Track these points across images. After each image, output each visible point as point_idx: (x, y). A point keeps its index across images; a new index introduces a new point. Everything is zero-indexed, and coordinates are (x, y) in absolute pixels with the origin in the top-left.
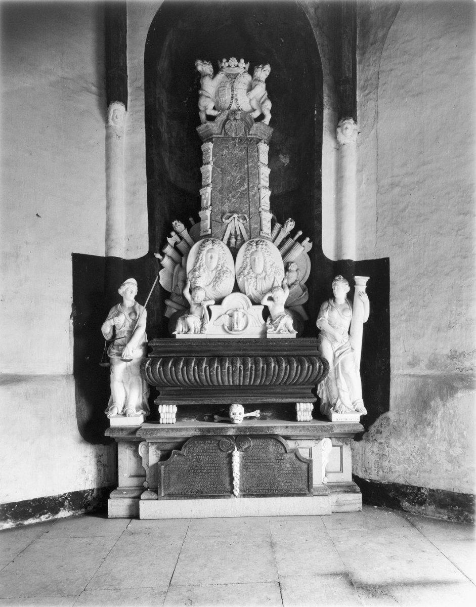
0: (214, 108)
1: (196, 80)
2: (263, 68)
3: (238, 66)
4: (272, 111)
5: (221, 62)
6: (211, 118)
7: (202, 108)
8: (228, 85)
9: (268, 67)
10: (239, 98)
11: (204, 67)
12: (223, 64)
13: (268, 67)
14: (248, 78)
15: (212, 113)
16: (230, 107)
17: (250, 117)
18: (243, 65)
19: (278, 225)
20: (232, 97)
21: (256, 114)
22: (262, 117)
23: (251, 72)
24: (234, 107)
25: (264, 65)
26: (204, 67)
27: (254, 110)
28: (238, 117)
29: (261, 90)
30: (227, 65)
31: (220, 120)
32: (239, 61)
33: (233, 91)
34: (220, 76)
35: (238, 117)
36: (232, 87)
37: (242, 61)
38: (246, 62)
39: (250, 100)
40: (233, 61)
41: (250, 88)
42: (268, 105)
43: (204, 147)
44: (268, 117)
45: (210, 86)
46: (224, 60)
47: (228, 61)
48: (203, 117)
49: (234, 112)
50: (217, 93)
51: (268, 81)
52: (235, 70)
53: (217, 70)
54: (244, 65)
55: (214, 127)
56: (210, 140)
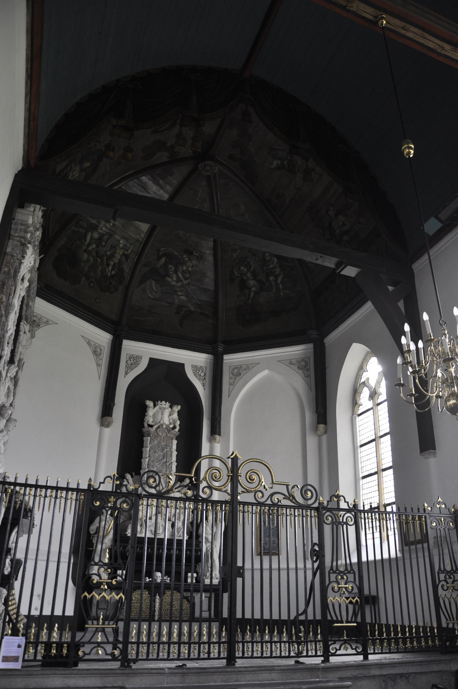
0: (152, 422)
1: (145, 409)
2: (177, 407)
3: (165, 405)
5: (158, 402)
7: (146, 421)
8: (160, 412)
9: (179, 407)
10: (165, 418)
11: (150, 403)
12: (158, 403)
13: (179, 407)
14: (170, 409)
16: (160, 422)
17: (169, 427)
18: (168, 404)
20: (162, 418)
21: (171, 426)
22: (174, 428)
23: (171, 407)
24: (162, 422)
25: (178, 405)
26: (150, 403)
27: (171, 424)
28: (164, 427)
29: (175, 416)
30: (160, 403)
31: (155, 427)
32: (166, 402)
33: (162, 415)
34: (157, 408)
36: (162, 413)
37: (168, 403)
38: (169, 403)
39: (170, 420)
40: (164, 402)
42: (178, 422)
45: (151, 412)
46: (159, 402)
47: (161, 402)
48: (146, 425)
49: (162, 425)
50: (154, 415)
51: (178, 412)
52: (164, 406)
53: (155, 406)
54: (168, 404)
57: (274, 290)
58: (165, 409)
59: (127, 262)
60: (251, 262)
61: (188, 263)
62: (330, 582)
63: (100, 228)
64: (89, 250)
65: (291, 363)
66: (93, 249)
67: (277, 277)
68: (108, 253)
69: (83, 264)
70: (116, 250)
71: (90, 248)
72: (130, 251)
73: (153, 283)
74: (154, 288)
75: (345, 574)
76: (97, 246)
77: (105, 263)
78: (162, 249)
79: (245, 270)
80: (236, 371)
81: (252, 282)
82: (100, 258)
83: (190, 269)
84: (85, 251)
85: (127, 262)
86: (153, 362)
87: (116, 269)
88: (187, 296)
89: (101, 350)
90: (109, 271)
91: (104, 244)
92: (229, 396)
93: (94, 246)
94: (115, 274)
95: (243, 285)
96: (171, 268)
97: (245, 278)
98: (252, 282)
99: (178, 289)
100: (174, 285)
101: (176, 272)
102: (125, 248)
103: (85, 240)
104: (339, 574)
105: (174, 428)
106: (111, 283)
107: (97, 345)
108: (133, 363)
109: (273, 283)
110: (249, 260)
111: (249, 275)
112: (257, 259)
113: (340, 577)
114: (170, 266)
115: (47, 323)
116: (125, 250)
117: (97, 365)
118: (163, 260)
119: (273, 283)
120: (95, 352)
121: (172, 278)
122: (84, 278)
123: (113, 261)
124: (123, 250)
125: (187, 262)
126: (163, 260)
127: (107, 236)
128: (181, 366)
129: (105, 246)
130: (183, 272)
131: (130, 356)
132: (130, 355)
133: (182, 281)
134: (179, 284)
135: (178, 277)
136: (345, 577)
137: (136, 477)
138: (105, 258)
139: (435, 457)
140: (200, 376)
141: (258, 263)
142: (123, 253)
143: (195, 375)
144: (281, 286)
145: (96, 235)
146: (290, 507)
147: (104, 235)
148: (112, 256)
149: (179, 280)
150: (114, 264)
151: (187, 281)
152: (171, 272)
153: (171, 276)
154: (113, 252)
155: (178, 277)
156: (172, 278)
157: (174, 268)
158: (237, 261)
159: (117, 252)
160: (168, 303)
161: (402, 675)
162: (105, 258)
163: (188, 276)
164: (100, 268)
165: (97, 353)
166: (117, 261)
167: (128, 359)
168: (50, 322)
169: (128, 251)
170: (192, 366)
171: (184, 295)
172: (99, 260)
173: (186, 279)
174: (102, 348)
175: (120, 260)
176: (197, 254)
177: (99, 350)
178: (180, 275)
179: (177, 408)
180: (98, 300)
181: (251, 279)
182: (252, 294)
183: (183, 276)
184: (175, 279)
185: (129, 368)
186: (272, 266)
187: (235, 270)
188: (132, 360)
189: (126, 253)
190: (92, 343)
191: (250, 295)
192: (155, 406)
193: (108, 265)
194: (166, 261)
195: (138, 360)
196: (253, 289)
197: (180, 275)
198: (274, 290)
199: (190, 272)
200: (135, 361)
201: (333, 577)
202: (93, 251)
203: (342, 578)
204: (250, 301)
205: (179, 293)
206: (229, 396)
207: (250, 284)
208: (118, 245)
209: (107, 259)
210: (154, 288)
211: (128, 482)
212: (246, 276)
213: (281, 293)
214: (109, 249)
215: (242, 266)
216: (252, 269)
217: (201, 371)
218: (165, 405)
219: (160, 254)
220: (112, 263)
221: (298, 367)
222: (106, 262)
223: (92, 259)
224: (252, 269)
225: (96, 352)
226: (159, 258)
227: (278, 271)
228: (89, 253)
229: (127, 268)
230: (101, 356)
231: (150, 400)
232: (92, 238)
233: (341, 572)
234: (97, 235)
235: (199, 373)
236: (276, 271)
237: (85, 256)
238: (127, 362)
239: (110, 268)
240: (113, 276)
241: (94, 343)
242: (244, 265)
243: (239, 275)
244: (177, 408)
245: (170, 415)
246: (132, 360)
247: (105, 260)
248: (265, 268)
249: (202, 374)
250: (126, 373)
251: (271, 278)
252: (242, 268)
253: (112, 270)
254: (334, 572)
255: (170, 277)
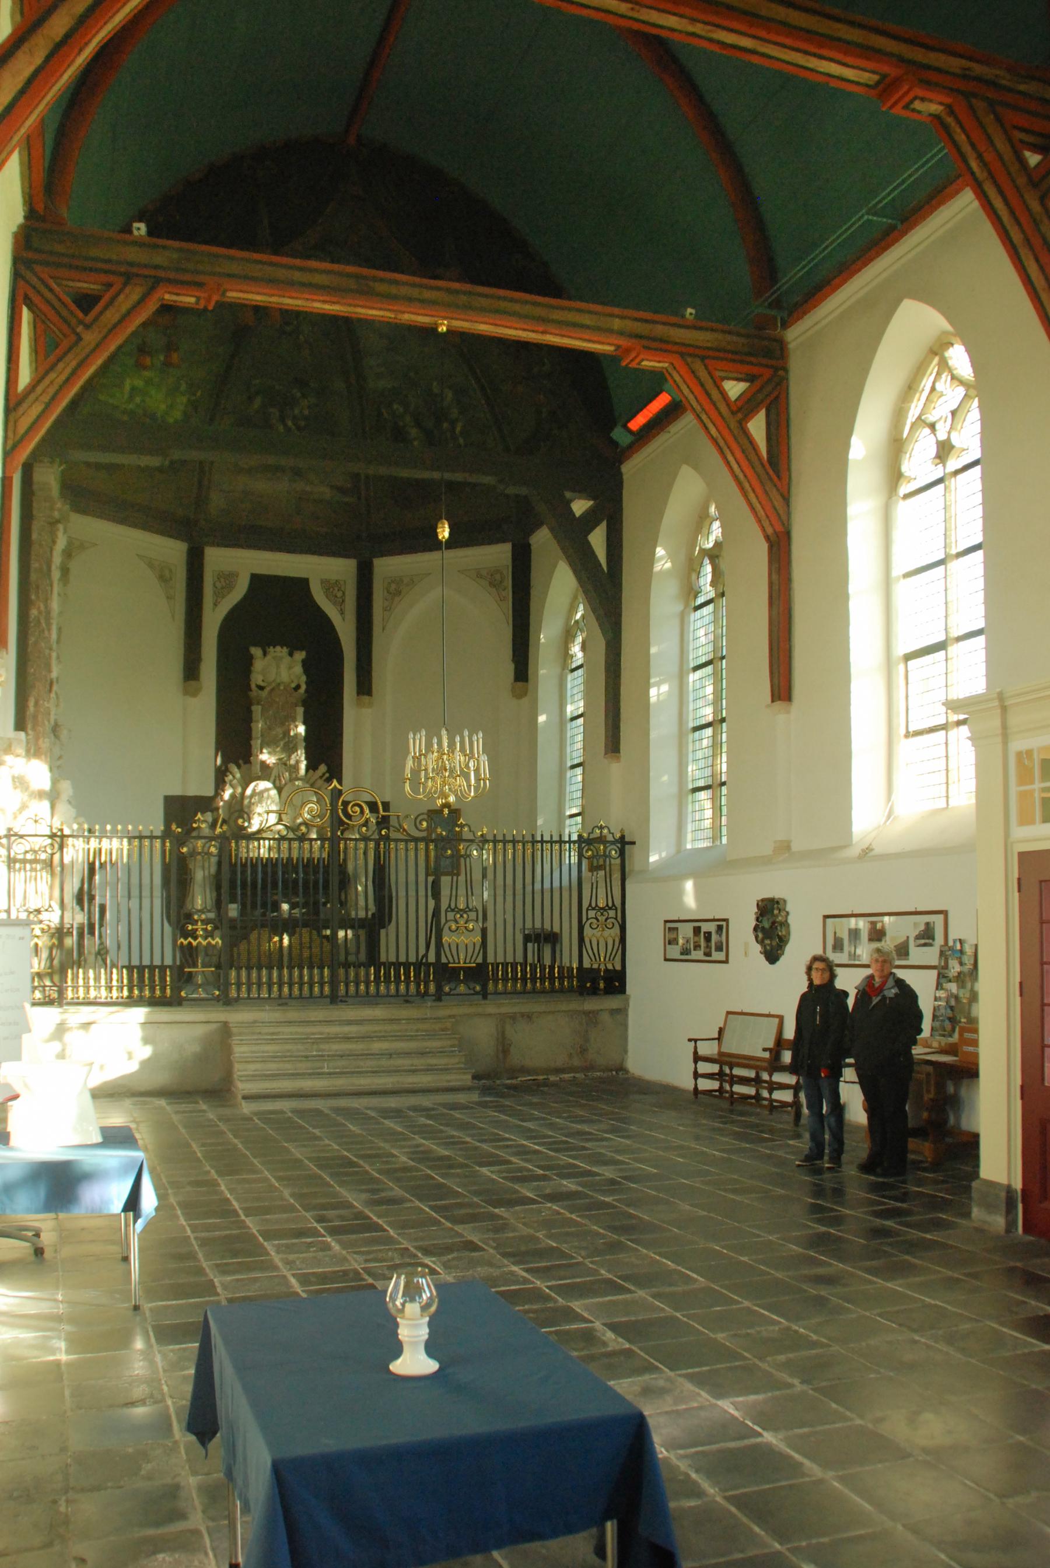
1: (249, 660)
4: (306, 683)
6: (261, 688)
11: (256, 652)
14: (289, 658)
15: (262, 684)
18: (285, 650)
19: (311, 771)
22: (298, 687)
23: (291, 654)
24: (278, 681)
26: (256, 652)
28: (282, 688)
29: (298, 669)
34: (269, 657)
35: (282, 688)
40: (278, 648)
41: (290, 668)
42: (304, 678)
43: (254, 708)
44: (304, 687)
45: (258, 665)
48: (253, 686)
52: (279, 654)
53: (265, 654)
55: (264, 694)
56: (258, 704)
58: (281, 658)
62: (447, 921)
65: (479, 576)
67: (453, 423)
75: (465, 912)
79: (401, 410)
80: (393, 586)
81: (414, 432)
83: (306, 412)
86: (258, 581)
89: (171, 571)
92: (383, 629)
98: (414, 432)
101: (282, 419)
104: (458, 912)
105: (298, 687)
108: (224, 584)
111: (408, 418)
113: (458, 916)
114: (271, 410)
117: (168, 598)
118: (258, 402)
120: (162, 578)
126: (258, 402)
128: (303, 584)
136: (465, 916)
137: (244, 767)
139: (618, 759)
140: (336, 596)
143: (327, 597)
146: (402, 840)
157: (278, 414)
161: (523, 1015)
163: (302, 423)
170: (322, 582)
178: (290, 423)
179: (300, 656)
185: (220, 594)
188: (222, 580)
192: (265, 654)
197: (290, 423)
201: (450, 915)
203: (462, 916)
206: (383, 629)
211: (234, 777)
217: (336, 589)
218: (281, 651)
221: (490, 583)
225: (164, 578)
226: (250, 399)
227: (455, 413)
231: (255, 645)
232: (133, 389)
233: (461, 910)
235: (335, 592)
244: (300, 656)
245: (290, 668)
246: (222, 580)
249: (339, 594)
250: (215, 605)
251: (445, 425)
252: (395, 406)
254: (453, 910)
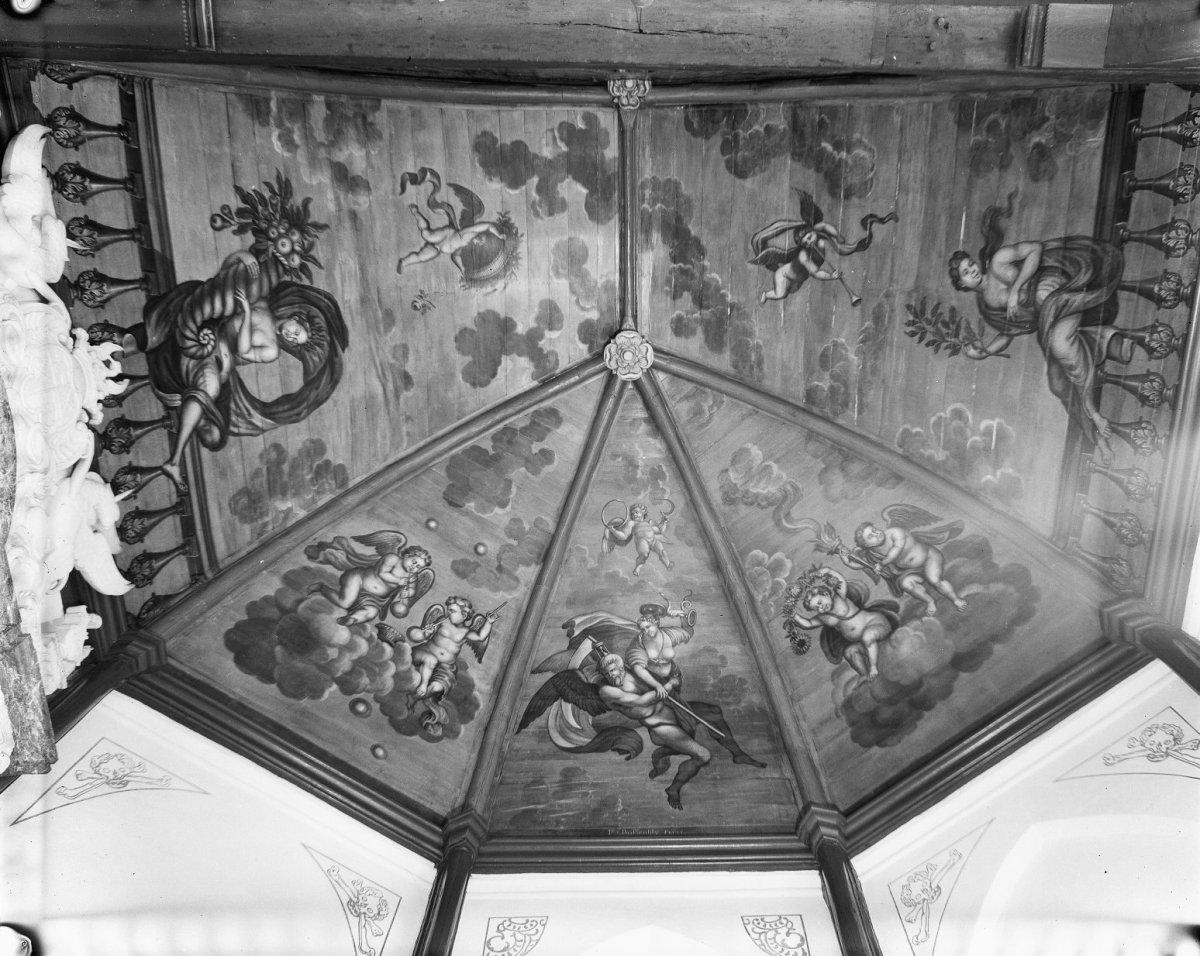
57: (932, 608)
59: (480, 661)
60: (832, 573)
61: (659, 639)
63: (385, 568)
64: (356, 620)
66: (368, 620)
67: (921, 571)
68: (418, 635)
69: (333, 653)
70: (440, 626)
71: (359, 616)
72: (484, 633)
73: (568, 708)
74: (573, 723)
76: (382, 615)
77: (408, 657)
78: (578, 621)
79: (826, 600)
82: (391, 645)
83: (670, 653)
84: (343, 621)
85: (480, 661)
87: (446, 678)
88: (678, 724)
89: (383, 903)
90: (421, 681)
91: (401, 609)
93: (372, 612)
94: (441, 693)
95: (835, 640)
96: (612, 662)
97: (832, 621)
99: (647, 712)
100: (631, 703)
101: (630, 670)
102: (468, 623)
103: (342, 595)
106: (430, 714)
107: (366, 884)
109: (920, 591)
110: (824, 571)
111: (841, 608)
112: (846, 559)
114: (609, 657)
115: (162, 784)
116: (471, 630)
118: (587, 647)
119: (920, 591)
121: (620, 686)
122: (335, 687)
123: (435, 656)
124: (465, 631)
125: (655, 636)
126: (587, 647)
127: (411, 592)
129: (405, 615)
130: (651, 665)
131: (502, 924)
132: (501, 921)
133: (652, 688)
134: (648, 696)
135: (638, 679)
138: (408, 646)
141: (853, 564)
142: (465, 638)
144: (946, 587)
145: (375, 586)
147: (400, 588)
148: (433, 639)
149: (642, 687)
150: (439, 664)
151: (669, 686)
152: (616, 673)
153: (618, 682)
154: (431, 632)
155: (638, 679)
156: (620, 686)
157: (621, 663)
158: (796, 590)
159: (445, 631)
160: (621, 752)
162: (408, 646)
163: (666, 671)
164: (392, 669)
165: (363, 910)
166: (447, 657)
167: (492, 932)
168: (175, 783)
169: (478, 633)
171: (666, 721)
172: (388, 649)
173: (663, 680)
174: (387, 896)
175: (457, 655)
176: (679, 612)
177: (373, 903)
178: (645, 675)
180: (380, 752)
181: (850, 614)
182: (872, 651)
183: (651, 673)
184: (629, 683)
186: (893, 554)
187: (797, 618)
189: (473, 637)
190: (348, 877)
191: (865, 655)
193: (418, 664)
194: (595, 647)
195: (534, 931)
196: (869, 636)
198: (932, 608)
199: (671, 661)
200: (520, 936)
202: (368, 625)
204: (874, 671)
205: (652, 721)
207: (853, 629)
208: (447, 616)
209: (414, 650)
210: (573, 722)
212: (833, 615)
213: (959, 603)
214: (419, 626)
215: (814, 595)
216: (843, 590)
219: (577, 633)
220: (430, 661)
222: (413, 655)
223: (363, 647)
224: (843, 590)
226: (574, 645)
227: (917, 555)
228: (358, 628)
229: (481, 677)
230: (384, 924)
232: (363, 593)
234: (376, 585)
235: (779, 939)
236: (912, 559)
237: (342, 635)
238: (487, 943)
239: (427, 673)
240: (437, 697)
241: (355, 877)
242: (816, 591)
243: (815, 623)
247: (409, 652)
248: (878, 567)
251: (908, 582)
252: (814, 602)
253: (431, 680)
255: (615, 686)
